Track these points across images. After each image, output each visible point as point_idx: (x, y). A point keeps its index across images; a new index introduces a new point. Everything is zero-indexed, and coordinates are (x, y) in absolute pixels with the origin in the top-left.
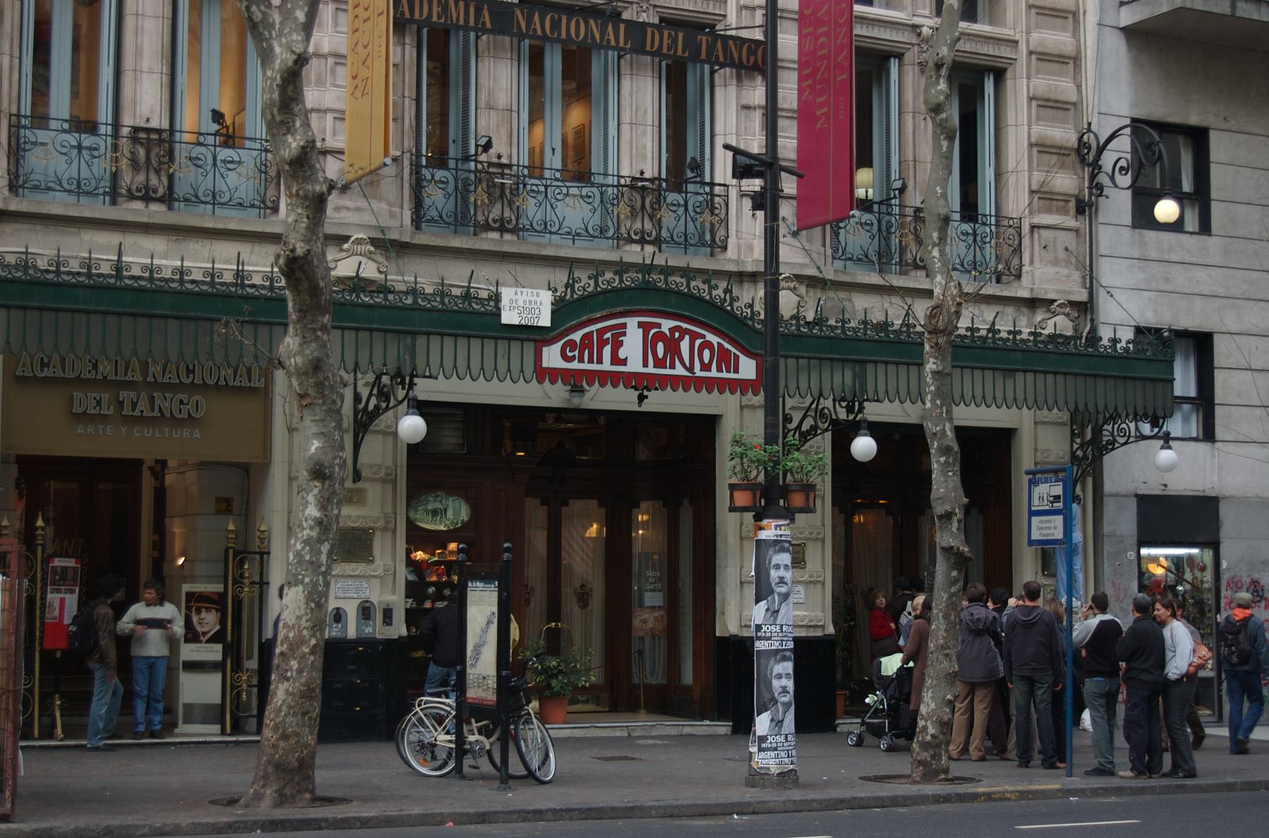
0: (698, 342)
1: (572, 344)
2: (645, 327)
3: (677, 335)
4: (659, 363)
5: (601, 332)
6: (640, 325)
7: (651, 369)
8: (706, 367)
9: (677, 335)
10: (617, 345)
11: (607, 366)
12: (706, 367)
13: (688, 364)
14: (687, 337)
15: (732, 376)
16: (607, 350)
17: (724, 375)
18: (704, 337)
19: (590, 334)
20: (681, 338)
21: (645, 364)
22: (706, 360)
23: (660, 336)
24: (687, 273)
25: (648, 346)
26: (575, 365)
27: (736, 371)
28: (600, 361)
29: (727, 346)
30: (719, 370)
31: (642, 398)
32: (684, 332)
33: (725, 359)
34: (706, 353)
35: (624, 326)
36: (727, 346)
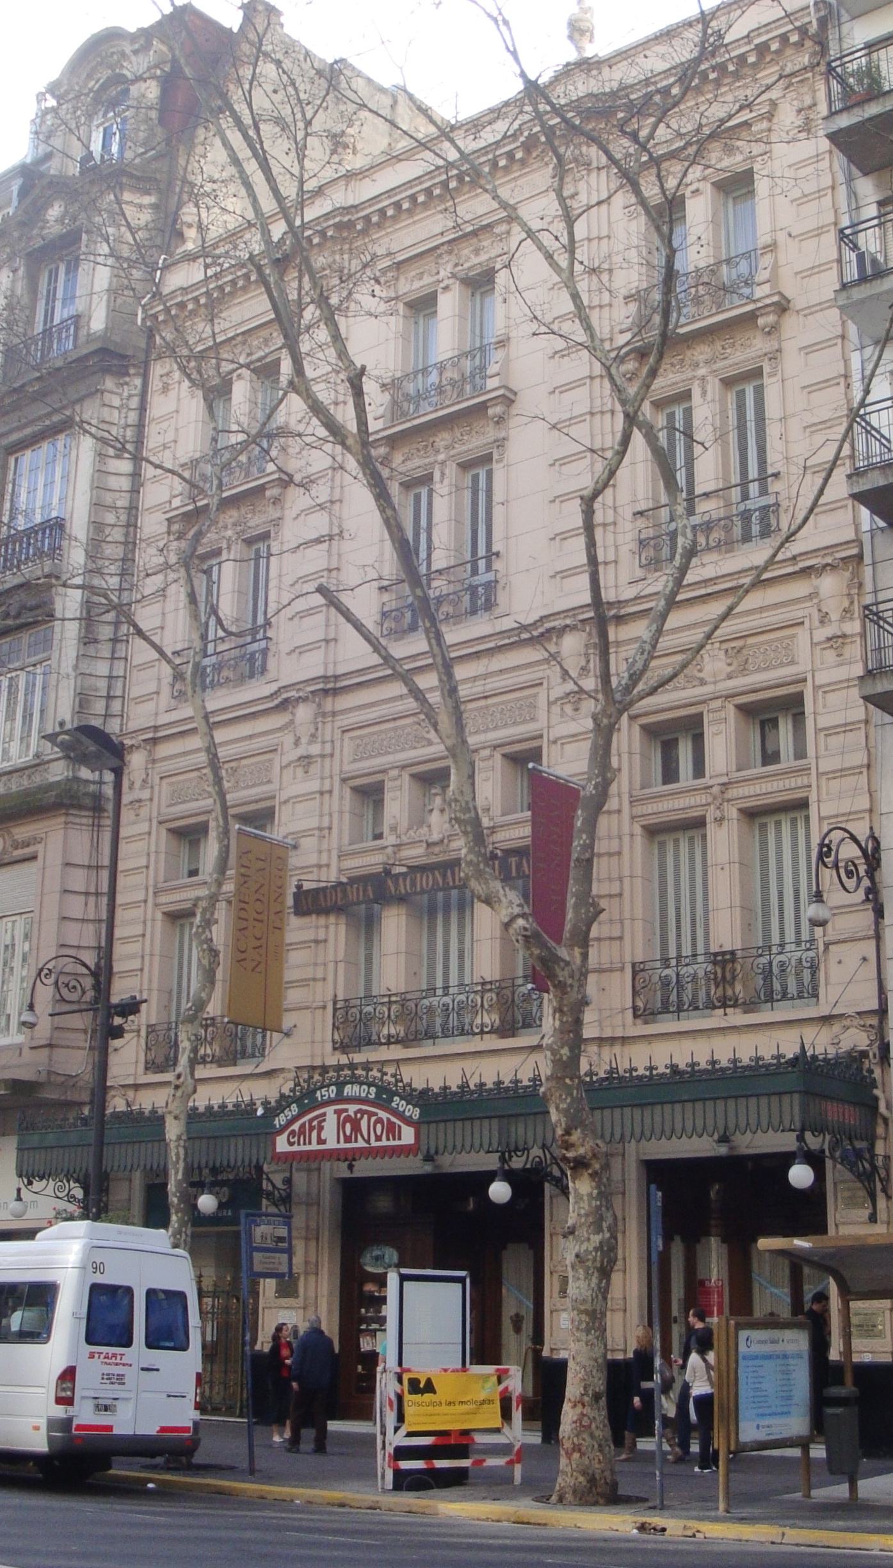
0: (373, 1119)
1: (293, 1133)
2: (338, 1112)
3: (359, 1116)
4: (348, 1140)
5: (311, 1121)
6: (336, 1112)
7: (343, 1145)
8: (378, 1138)
9: (359, 1116)
10: (321, 1129)
11: (315, 1146)
12: (378, 1138)
13: (366, 1137)
14: (366, 1116)
15: (397, 1143)
16: (314, 1134)
17: (392, 1143)
18: (376, 1114)
19: (304, 1124)
20: (362, 1117)
21: (338, 1142)
22: (379, 1133)
23: (348, 1119)
24: (367, 1066)
25: (340, 1126)
26: (295, 1148)
27: (400, 1139)
28: (310, 1143)
29: (393, 1119)
30: (388, 1139)
31: (351, 1167)
32: (363, 1112)
33: (392, 1130)
34: (379, 1126)
35: (324, 1114)
36: (393, 1119)
